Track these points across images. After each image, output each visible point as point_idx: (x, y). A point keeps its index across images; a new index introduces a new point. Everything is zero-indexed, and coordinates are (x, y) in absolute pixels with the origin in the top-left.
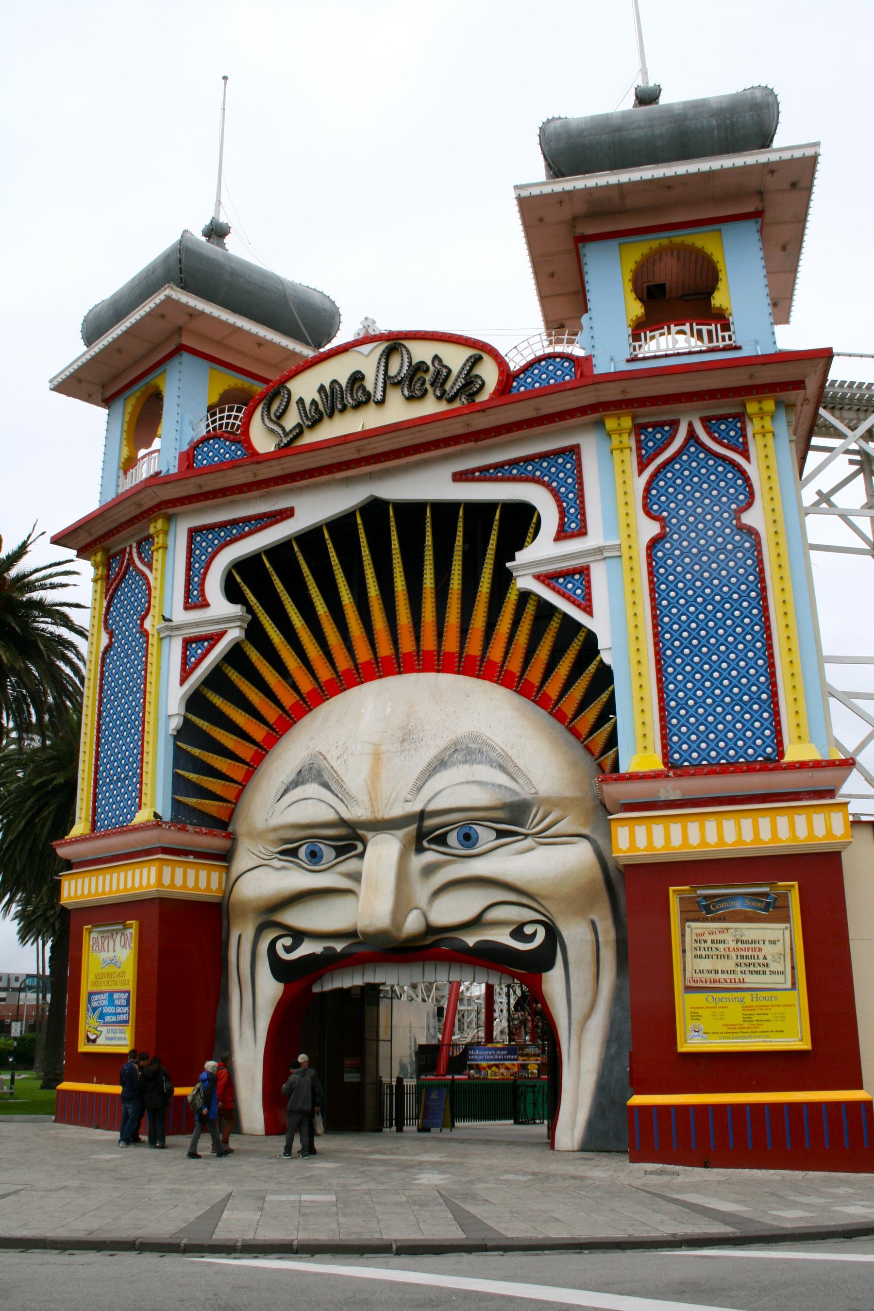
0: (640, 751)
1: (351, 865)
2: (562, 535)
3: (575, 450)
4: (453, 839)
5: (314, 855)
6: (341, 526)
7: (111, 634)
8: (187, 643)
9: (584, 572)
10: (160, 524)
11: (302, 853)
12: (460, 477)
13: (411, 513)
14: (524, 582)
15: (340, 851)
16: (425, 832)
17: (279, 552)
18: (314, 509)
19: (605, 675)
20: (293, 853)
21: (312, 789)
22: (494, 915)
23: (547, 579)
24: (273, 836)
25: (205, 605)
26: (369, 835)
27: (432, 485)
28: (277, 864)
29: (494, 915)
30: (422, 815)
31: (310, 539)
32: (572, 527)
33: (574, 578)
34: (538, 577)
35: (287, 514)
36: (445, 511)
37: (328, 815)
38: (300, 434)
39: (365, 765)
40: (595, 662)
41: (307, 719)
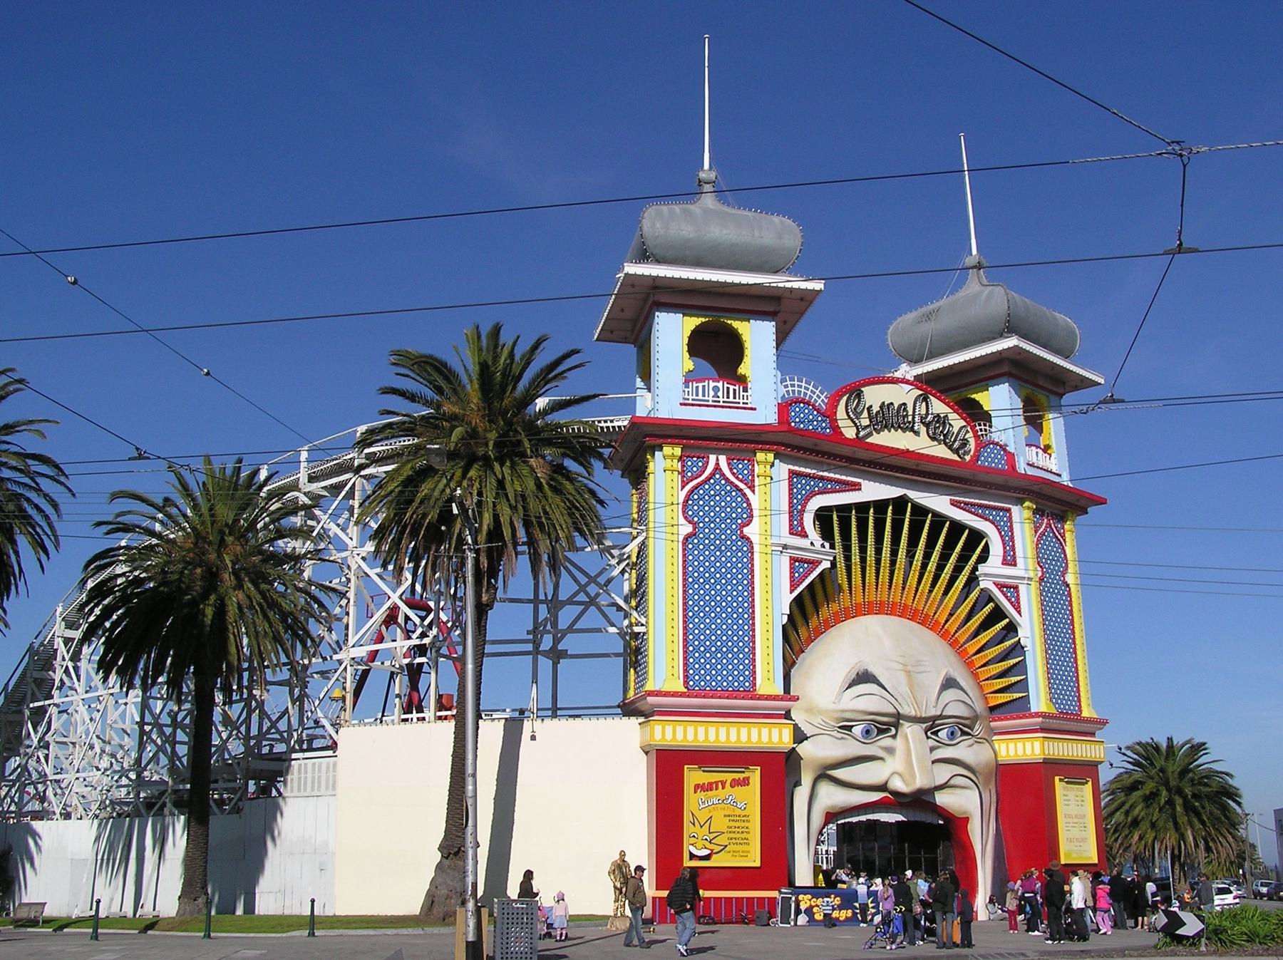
0: (1040, 701)
1: (886, 741)
2: (1005, 562)
3: (1009, 510)
4: (943, 734)
5: (868, 732)
6: (880, 506)
7: (695, 524)
8: (793, 560)
9: (1016, 588)
10: (771, 456)
11: (858, 730)
12: (954, 503)
13: (920, 511)
14: (984, 584)
15: (881, 731)
16: (931, 725)
17: (844, 509)
18: (873, 491)
19: (1018, 648)
20: (849, 728)
21: (872, 687)
22: (952, 782)
23: (1000, 586)
24: (837, 715)
25: (804, 535)
26: (906, 724)
27: (939, 503)
28: (834, 733)
29: (952, 782)
30: (941, 717)
31: (862, 508)
32: (1009, 560)
33: (1010, 589)
34: (996, 584)
35: (856, 487)
36: (939, 520)
37: (892, 710)
38: (870, 434)
39: (902, 677)
40: (1012, 641)
41: (833, 632)
